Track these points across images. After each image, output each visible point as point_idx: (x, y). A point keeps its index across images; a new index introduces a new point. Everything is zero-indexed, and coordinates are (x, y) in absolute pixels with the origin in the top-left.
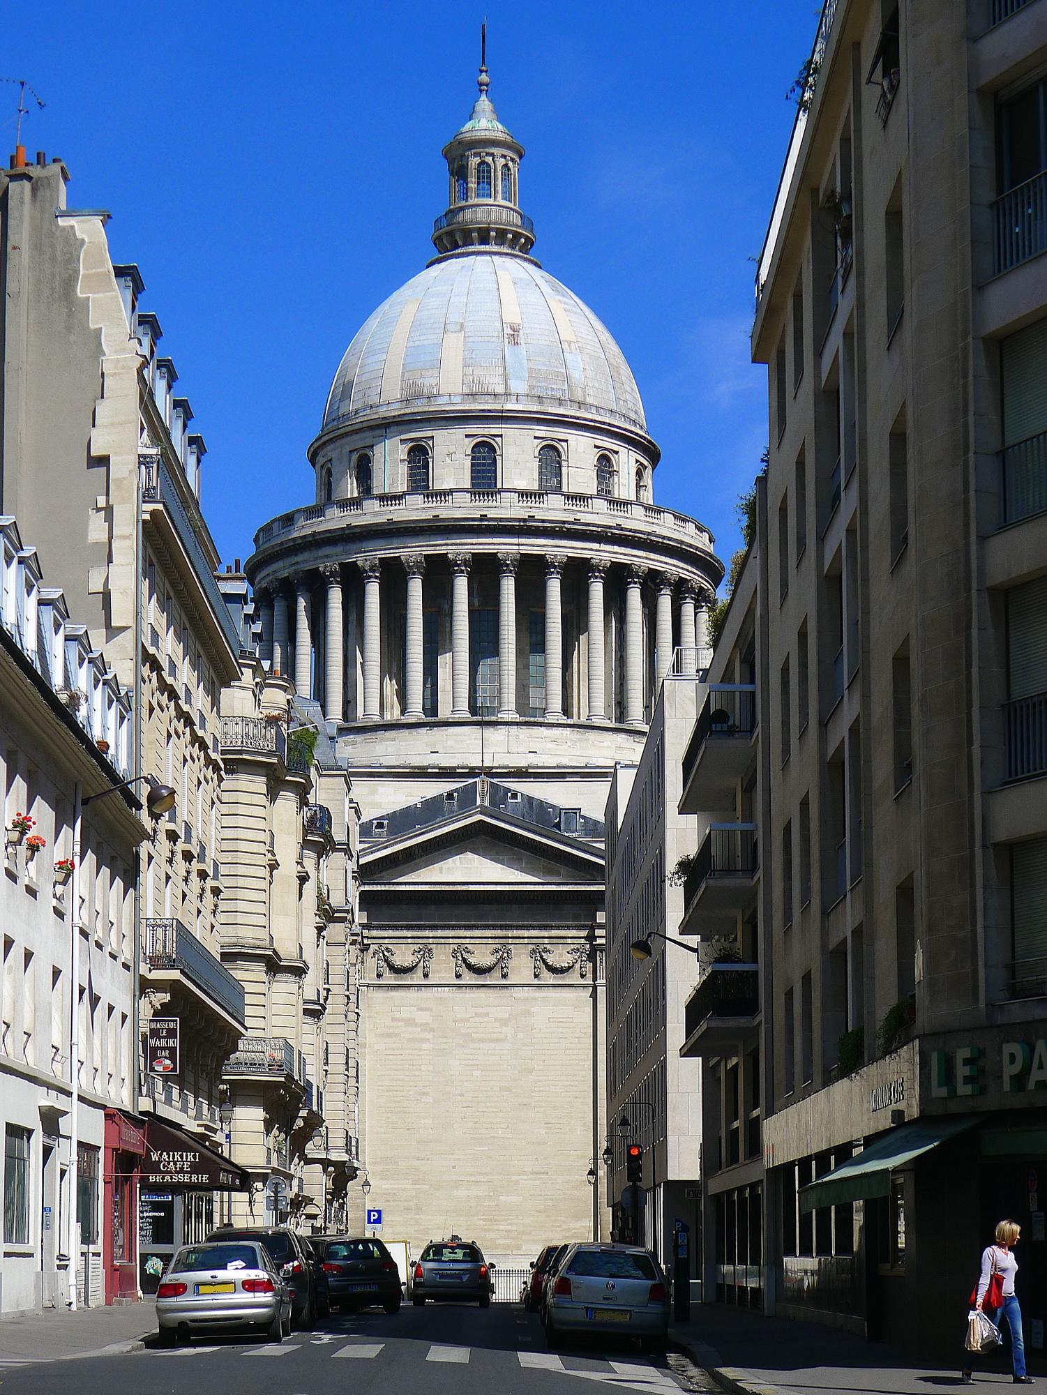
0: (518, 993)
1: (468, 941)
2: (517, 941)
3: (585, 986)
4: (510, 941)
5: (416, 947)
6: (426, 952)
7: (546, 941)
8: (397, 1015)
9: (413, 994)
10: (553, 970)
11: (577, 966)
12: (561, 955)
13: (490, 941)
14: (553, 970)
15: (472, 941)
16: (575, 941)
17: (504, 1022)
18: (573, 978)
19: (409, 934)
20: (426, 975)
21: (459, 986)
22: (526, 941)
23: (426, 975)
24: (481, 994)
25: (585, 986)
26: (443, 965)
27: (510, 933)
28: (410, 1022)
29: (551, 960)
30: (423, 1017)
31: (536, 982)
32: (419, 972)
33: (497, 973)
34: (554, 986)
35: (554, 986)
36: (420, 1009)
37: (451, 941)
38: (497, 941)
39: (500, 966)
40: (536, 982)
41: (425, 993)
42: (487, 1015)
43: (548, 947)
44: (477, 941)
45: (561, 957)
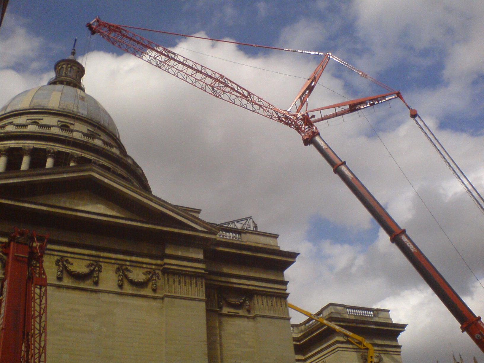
1: (69, 255)
2: (107, 260)
4: (101, 260)
7: (128, 263)
10: (132, 283)
12: (138, 275)
13: (86, 257)
14: (132, 283)
15: (72, 256)
16: (148, 266)
18: (147, 291)
22: (113, 261)
27: (102, 254)
29: (131, 276)
31: (119, 290)
37: (56, 253)
38: (91, 258)
40: (119, 290)
43: (129, 268)
44: (76, 256)
45: (138, 275)
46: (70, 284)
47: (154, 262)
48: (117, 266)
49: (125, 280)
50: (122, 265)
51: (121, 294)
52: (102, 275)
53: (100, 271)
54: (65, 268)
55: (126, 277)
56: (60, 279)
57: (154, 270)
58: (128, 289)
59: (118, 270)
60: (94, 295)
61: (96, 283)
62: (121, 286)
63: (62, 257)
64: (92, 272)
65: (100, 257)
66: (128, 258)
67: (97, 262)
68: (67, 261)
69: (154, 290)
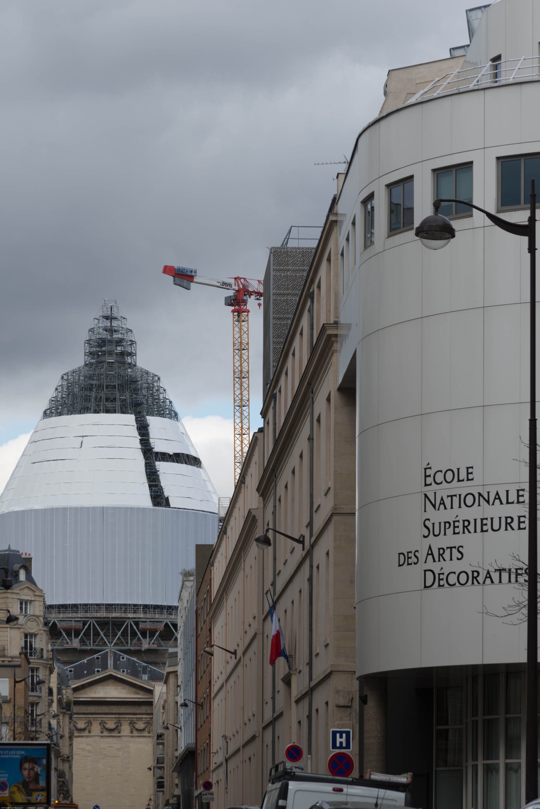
0: (124, 739)
3: (149, 737)
5: (86, 721)
6: (90, 723)
8: (78, 747)
9: (84, 739)
11: (147, 729)
17: (119, 750)
18: (146, 734)
19: (83, 716)
20: (90, 732)
21: (102, 736)
23: (90, 732)
24: (110, 740)
25: (149, 737)
26: (96, 728)
27: (121, 716)
28: (83, 749)
30: (88, 748)
31: (131, 735)
32: (87, 731)
33: (116, 732)
34: (138, 736)
35: (138, 736)
36: (87, 745)
39: (117, 729)
41: (88, 739)
42: (112, 747)
45: (140, 725)
46: (107, 735)
47: (148, 717)
48: (129, 721)
49: (134, 729)
50: (132, 721)
51: (132, 737)
52: (123, 727)
53: (121, 725)
54: (104, 726)
55: (134, 727)
56: (102, 732)
57: (149, 721)
58: (136, 733)
59: (130, 723)
60: (119, 739)
61: (119, 732)
62: (132, 732)
63: (102, 721)
64: (117, 727)
65: (120, 718)
66: (134, 716)
67: (119, 721)
68: (105, 723)
69: (149, 732)
